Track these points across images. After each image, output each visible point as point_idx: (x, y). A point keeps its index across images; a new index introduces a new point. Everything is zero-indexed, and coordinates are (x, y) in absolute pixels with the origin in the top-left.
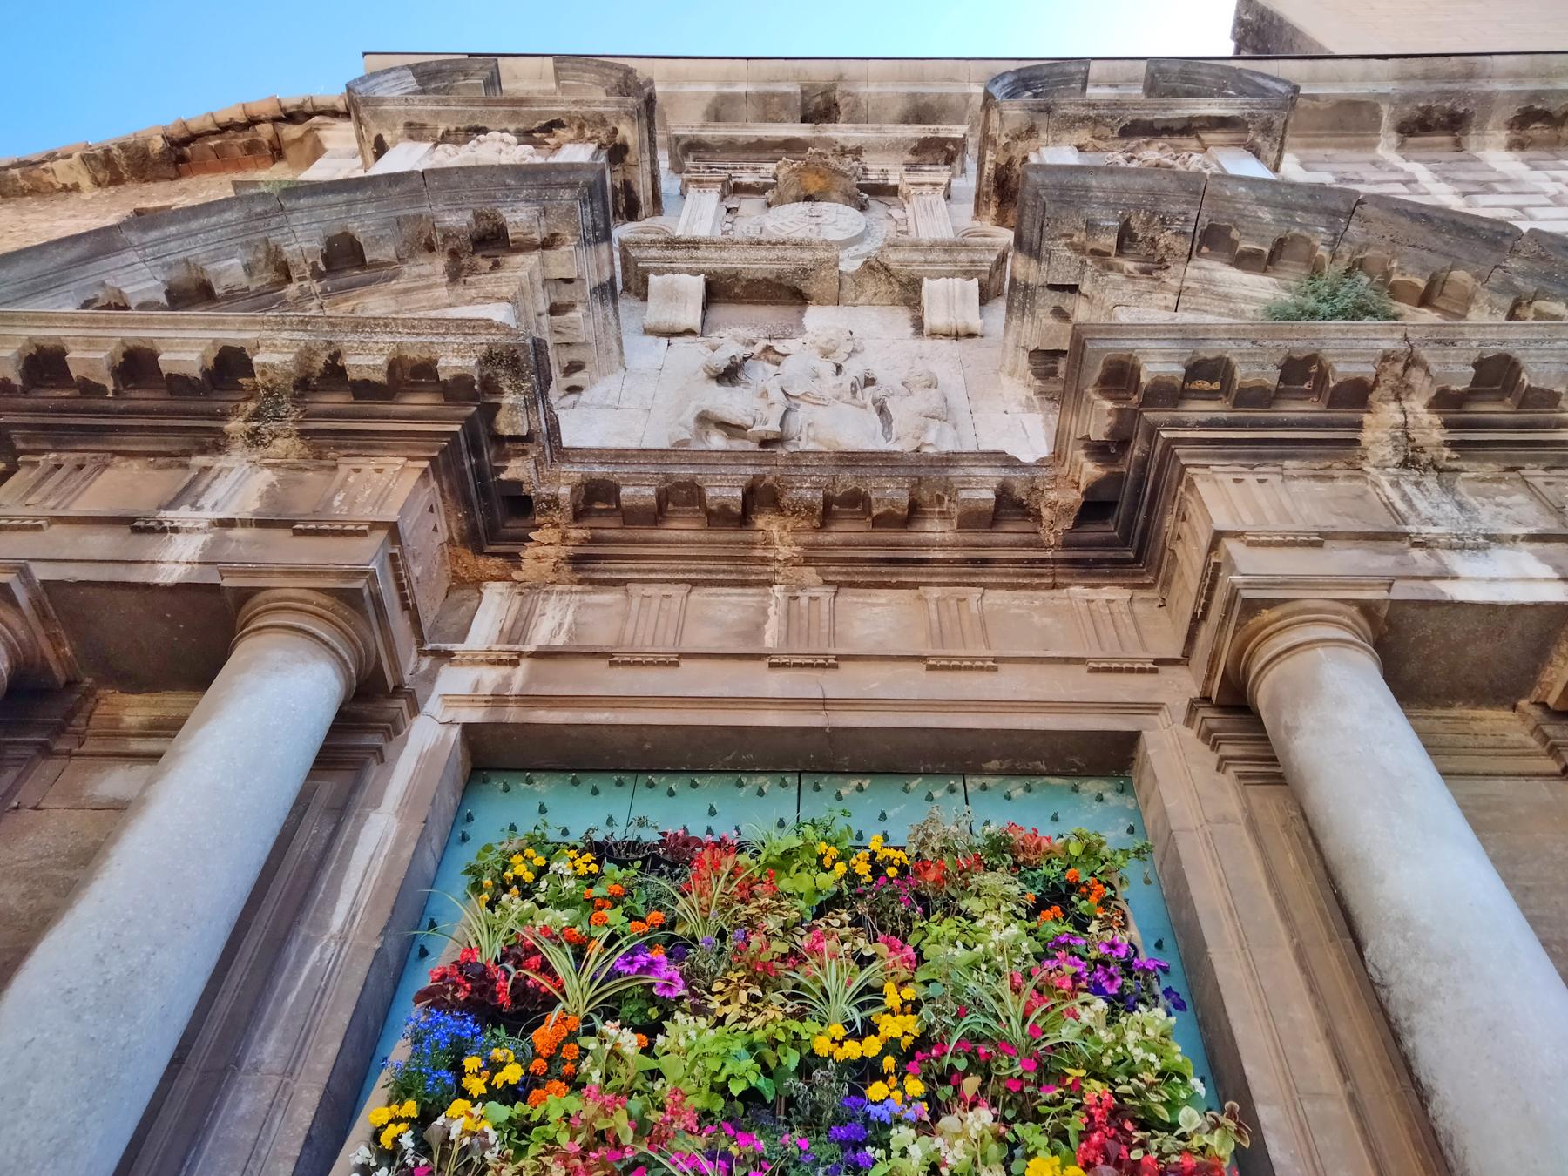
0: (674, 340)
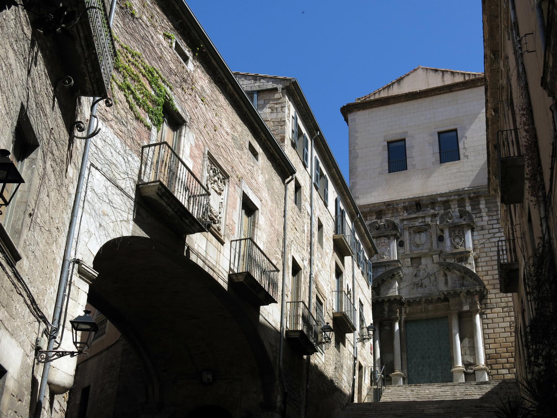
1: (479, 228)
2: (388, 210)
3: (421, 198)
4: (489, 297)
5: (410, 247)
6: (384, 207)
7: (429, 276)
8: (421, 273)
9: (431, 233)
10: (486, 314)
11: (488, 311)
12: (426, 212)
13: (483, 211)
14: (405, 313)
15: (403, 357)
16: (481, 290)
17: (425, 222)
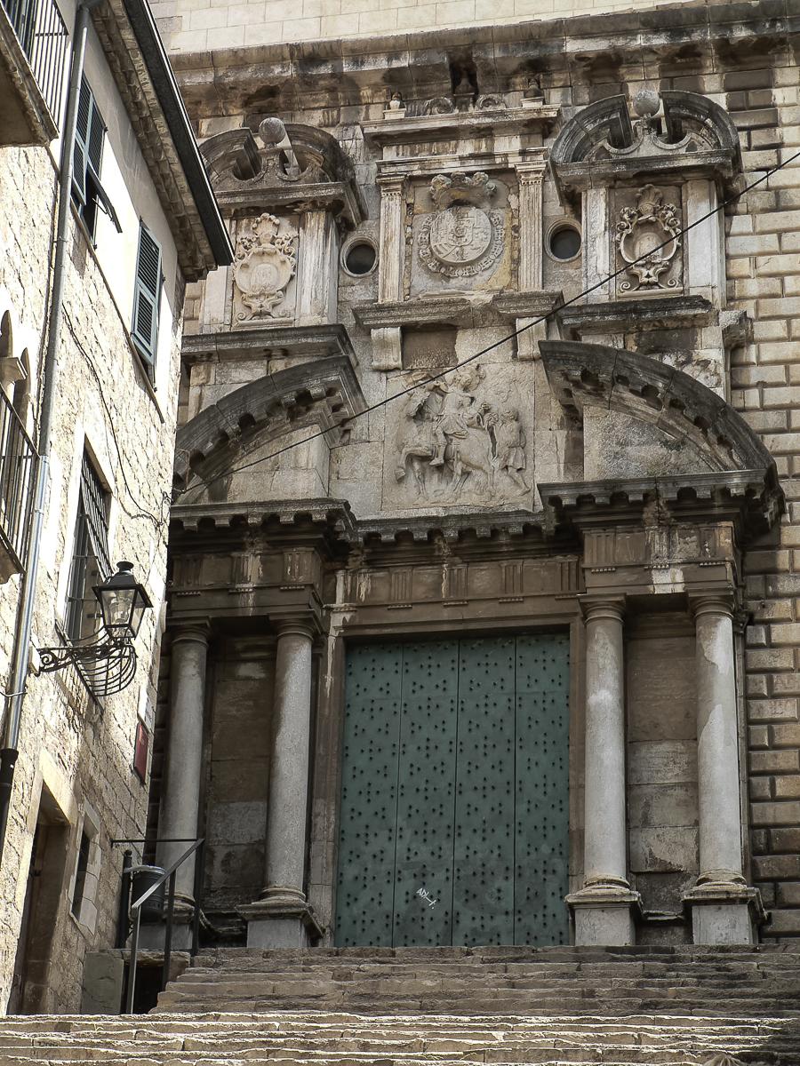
0: (391, 375)
1: (759, 200)
2: (309, 83)
3: (481, 36)
4: (786, 540)
5: (406, 272)
6: (290, 72)
7: (485, 420)
8: (450, 409)
9: (515, 214)
10: (768, 623)
11: (782, 608)
12: (499, 108)
13: (786, 116)
14: (350, 597)
15: (320, 823)
16: (750, 491)
17: (490, 156)
